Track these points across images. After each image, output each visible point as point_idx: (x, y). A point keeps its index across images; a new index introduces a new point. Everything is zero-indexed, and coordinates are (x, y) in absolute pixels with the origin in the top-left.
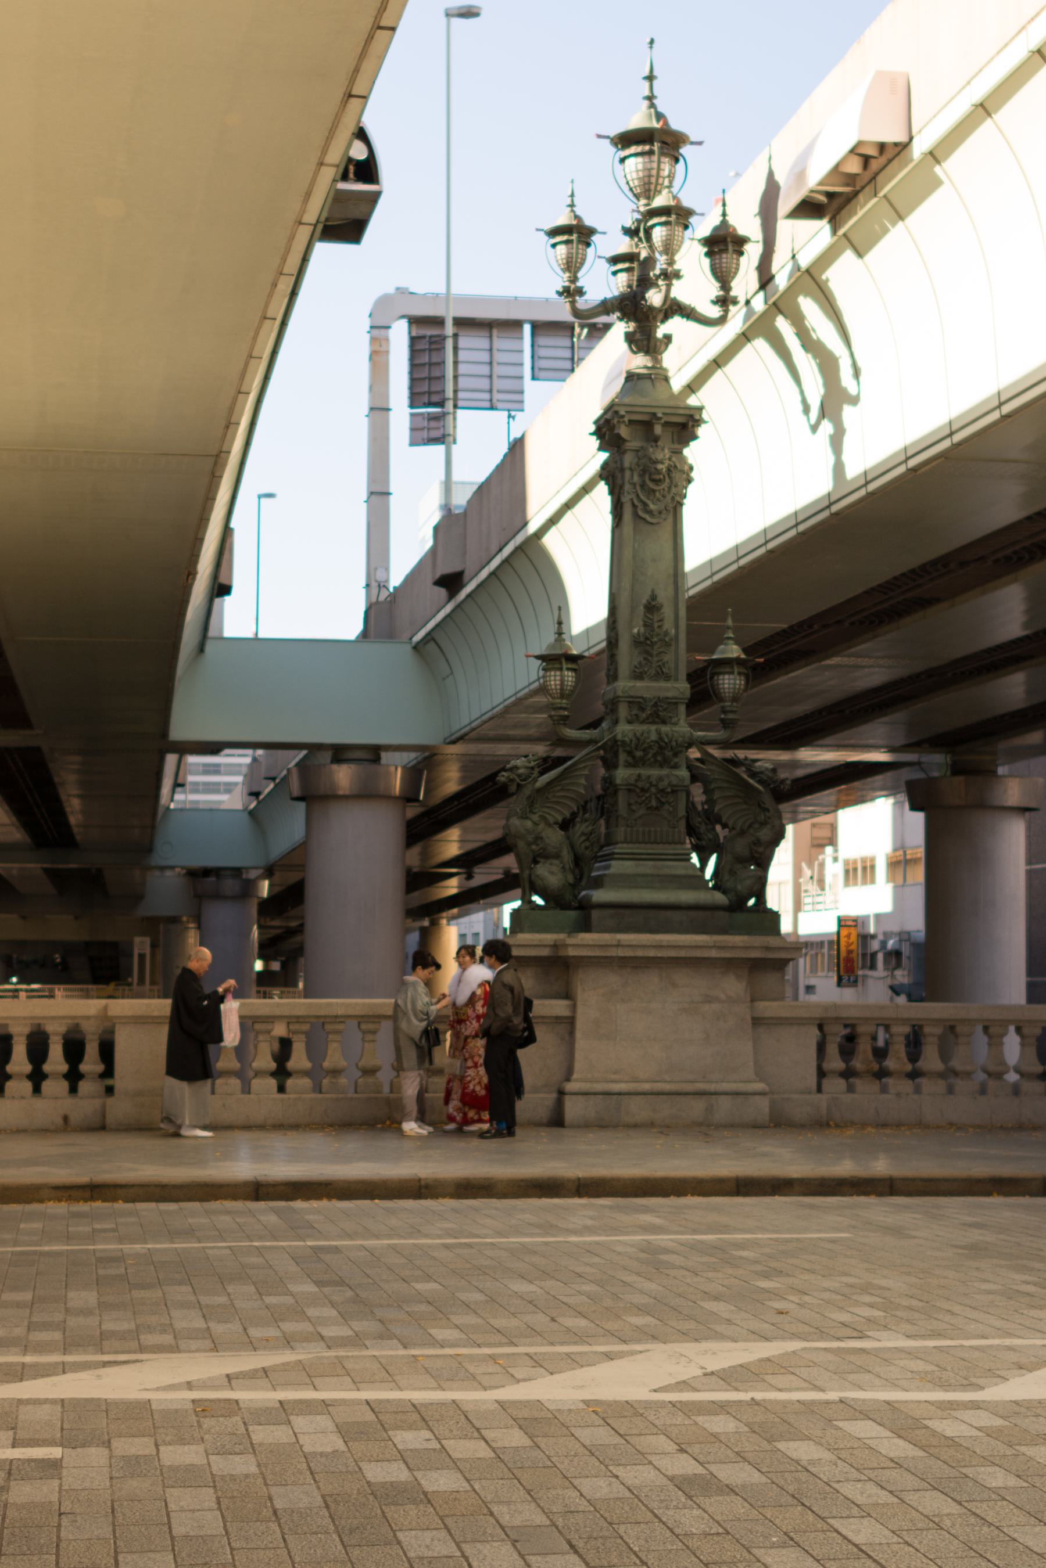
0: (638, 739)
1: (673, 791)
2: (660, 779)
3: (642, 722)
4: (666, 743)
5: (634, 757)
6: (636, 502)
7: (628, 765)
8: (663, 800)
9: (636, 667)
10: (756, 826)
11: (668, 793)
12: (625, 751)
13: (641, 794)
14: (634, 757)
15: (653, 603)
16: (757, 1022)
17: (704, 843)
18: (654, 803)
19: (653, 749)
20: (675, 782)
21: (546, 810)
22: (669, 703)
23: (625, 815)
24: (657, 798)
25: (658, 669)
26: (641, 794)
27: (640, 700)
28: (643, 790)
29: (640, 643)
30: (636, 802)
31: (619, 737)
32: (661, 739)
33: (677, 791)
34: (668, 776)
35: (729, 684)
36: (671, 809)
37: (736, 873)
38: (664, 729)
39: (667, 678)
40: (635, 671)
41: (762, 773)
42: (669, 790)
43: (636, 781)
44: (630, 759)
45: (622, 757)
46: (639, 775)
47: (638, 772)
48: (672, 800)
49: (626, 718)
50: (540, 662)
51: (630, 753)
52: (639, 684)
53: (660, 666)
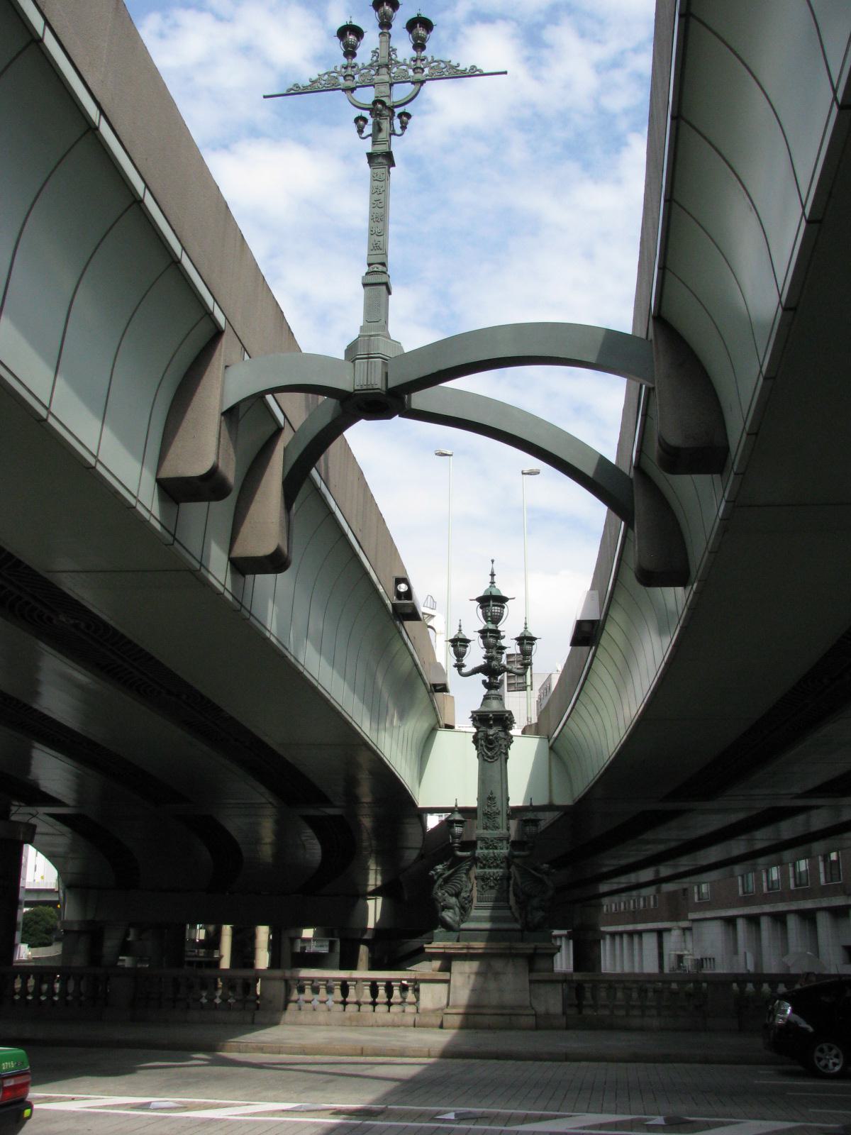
3: (487, 848)
6: (483, 753)
16: (531, 982)
18: (492, 884)
34: (497, 872)
38: (495, 851)
39: (498, 828)
44: (482, 865)
52: (485, 831)
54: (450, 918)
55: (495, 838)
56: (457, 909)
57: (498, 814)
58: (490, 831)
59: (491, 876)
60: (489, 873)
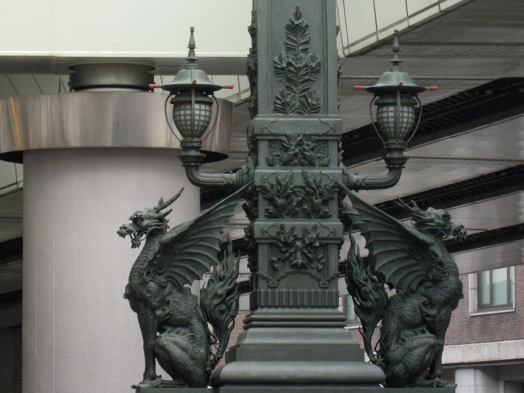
0: (279, 184)
1: (322, 245)
2: (306, 231)
3: (286, 164)
4: (314, 189)
5: (276, 206)
7: (270, 216)
8: (310, 256)
9: (277, 98)
10: (428, 284)
11: (316, 248)
12: (265, 198)
13: (284, 250)
14: (276, 206)
15: (296, 22)
17: (369, 304)
19: (297, 196)
20: (324, 234)
21: (176, 270)
22: (318, 141)
23: (266, 275)
24: (303, 254)
25: (303, 100)
26: (284, 250)
27: (284, 139)
28: (286, 244)
29: (282, 69)
30: (279, 259)
31: (258, 182)
32: (307, 183)
33: (327, 244)
34: (315, 228)
35: (408, 118)
36: (321, 267)
37: (404, 341)
38: (311, 172)
39: (314, 110)
40: (275, 103)
41: (432, 221)
42: (317, 244)
43: (278, 234)
44: (271, 209)
45: (263, 205)
46: (282, 227)
47: (280, 223)
48: (321, 256)
49: (267, 159)
50: (168, 93)
51: (271, 201)
52: (281, 119)
53: (305, 96)
54: (184, 349)
55: (308, 137)
56: (197, 326)
57: (315, 71)
58: (293, 118)
59: (296, 238)
60: (293, 229)
